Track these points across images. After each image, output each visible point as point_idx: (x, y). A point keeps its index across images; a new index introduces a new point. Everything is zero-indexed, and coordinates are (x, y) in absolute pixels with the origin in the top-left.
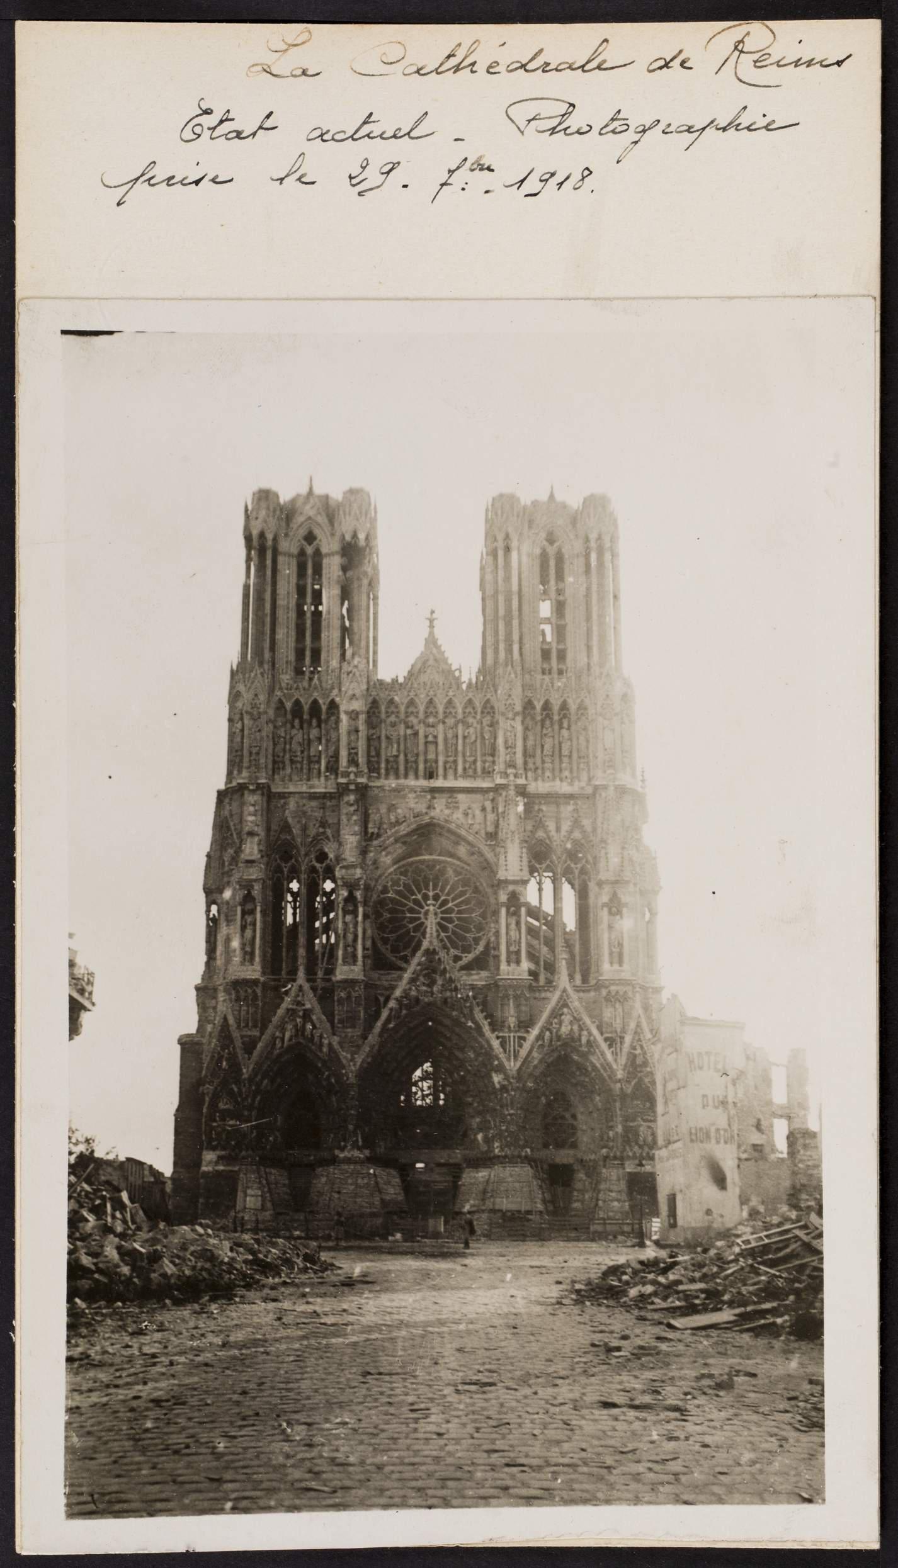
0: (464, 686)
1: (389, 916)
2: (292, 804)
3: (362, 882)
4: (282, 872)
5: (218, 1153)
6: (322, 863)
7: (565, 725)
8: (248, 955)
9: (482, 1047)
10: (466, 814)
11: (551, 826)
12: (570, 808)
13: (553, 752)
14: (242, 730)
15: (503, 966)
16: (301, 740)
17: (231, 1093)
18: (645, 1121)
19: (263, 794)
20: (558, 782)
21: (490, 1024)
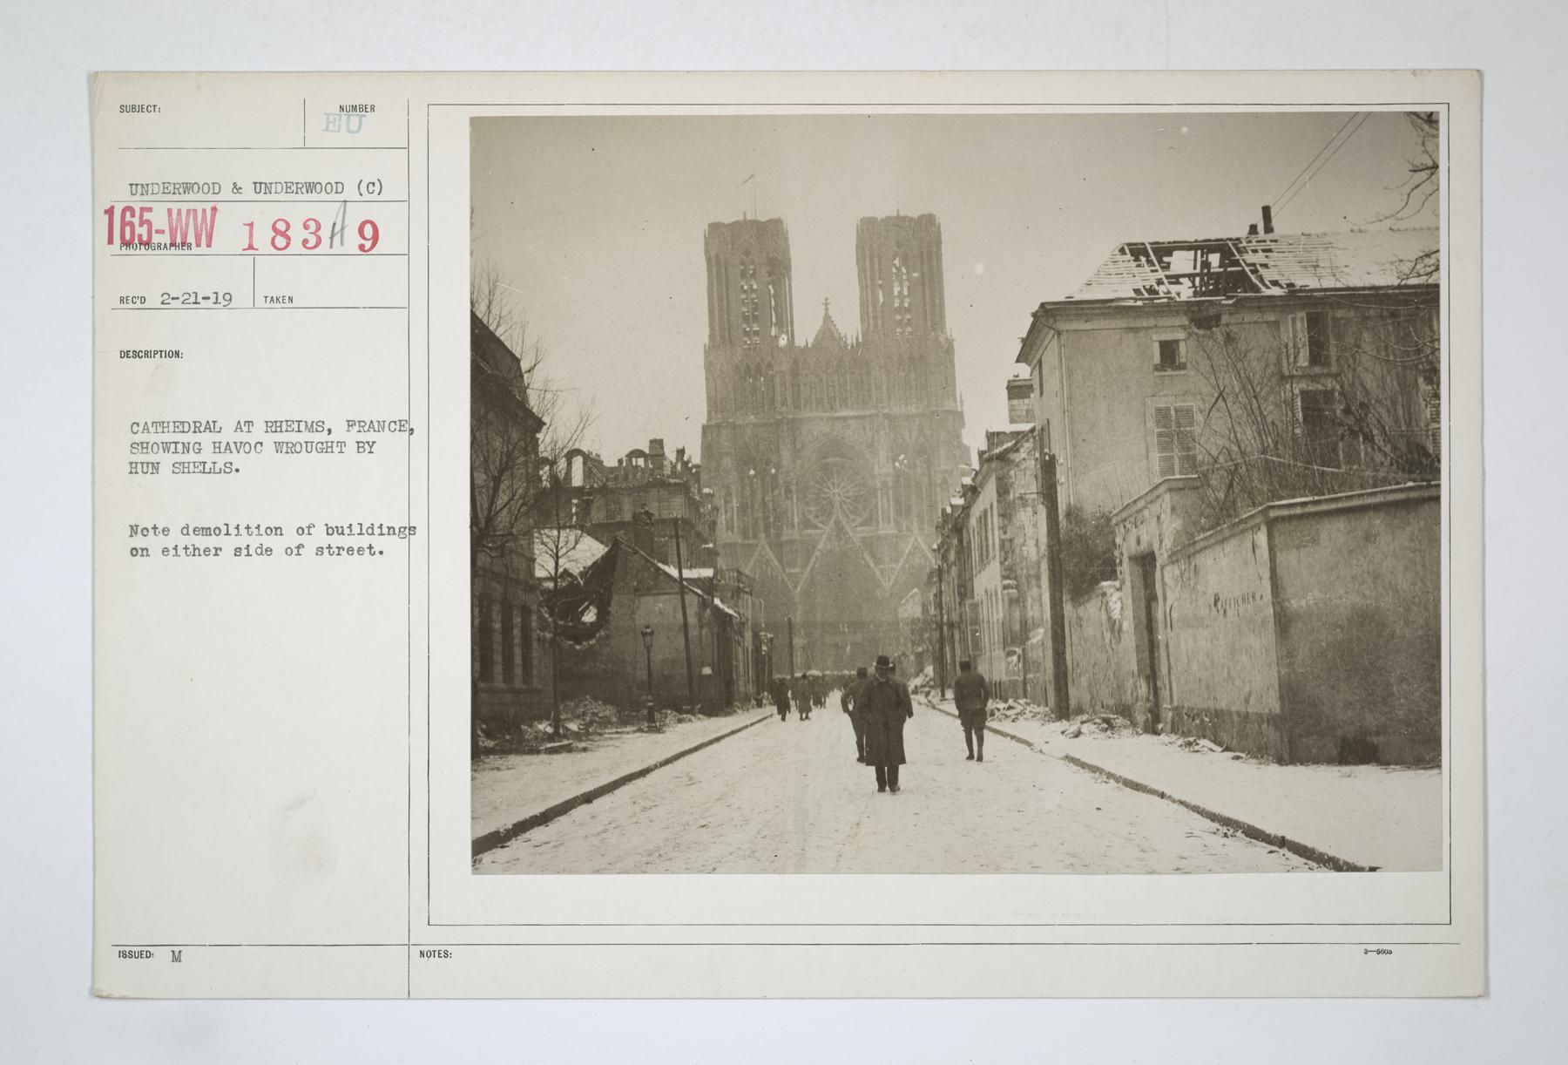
0: (849, 347)
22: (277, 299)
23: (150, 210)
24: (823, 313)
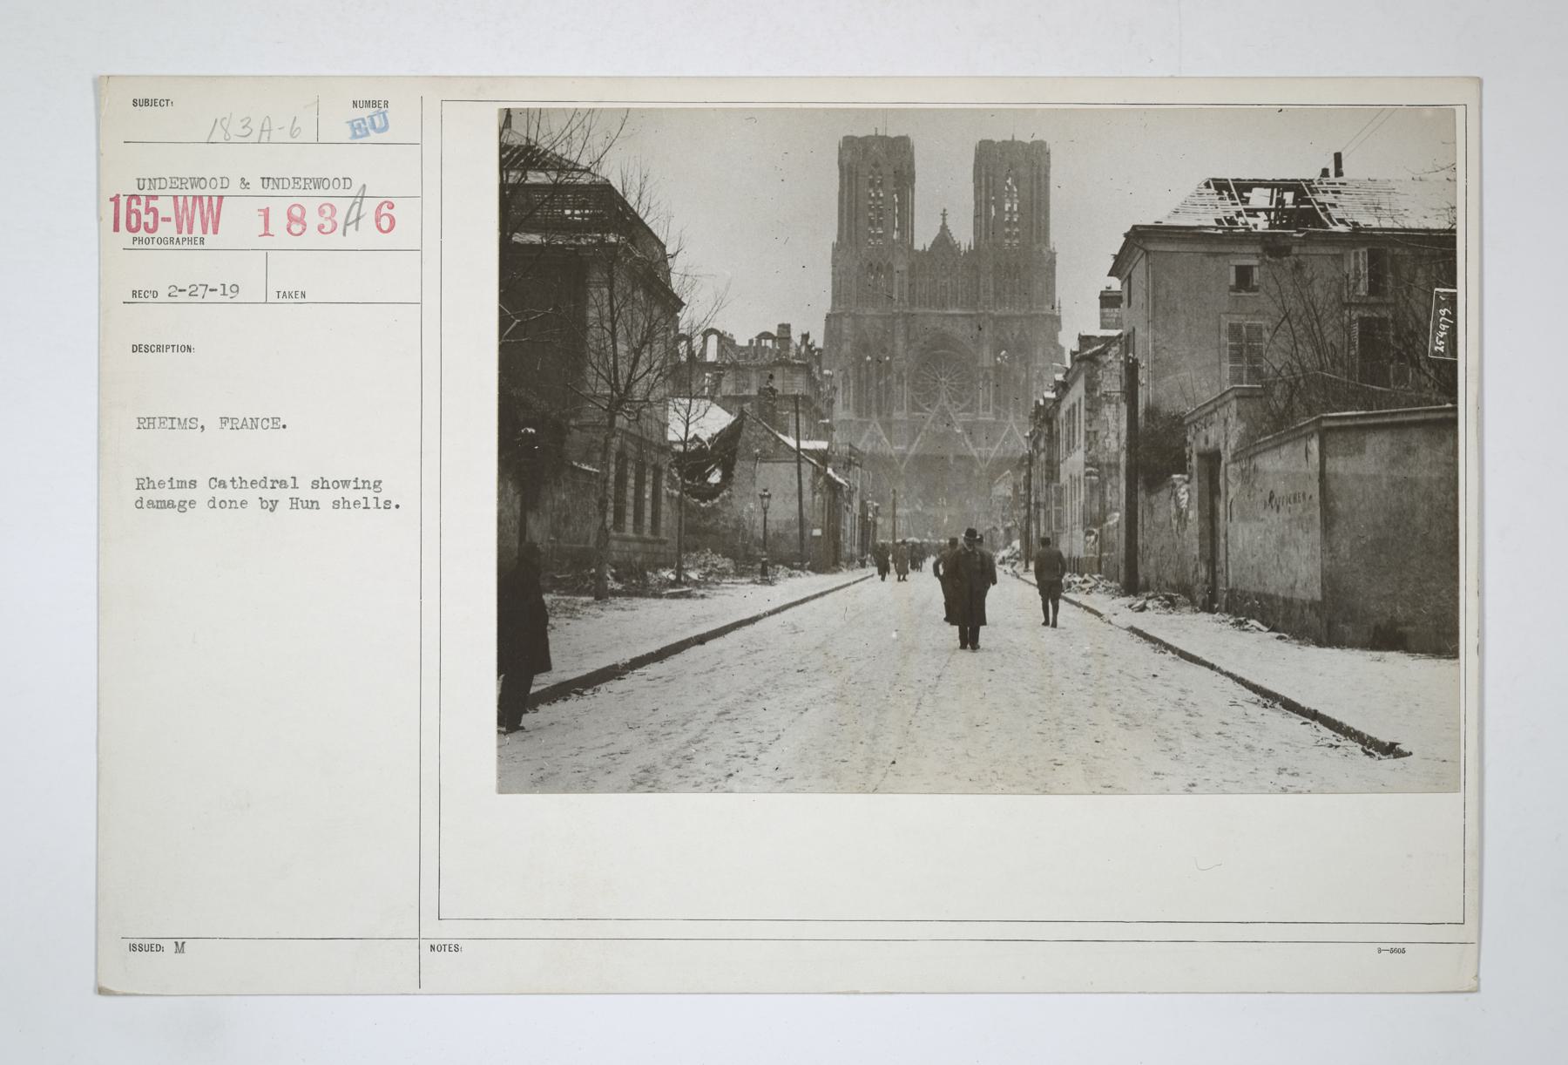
2: (867, 321)
3: (906, 368)
11: (1008, 334)
12: (1019, 324)
14: (840, 281)
22: (290, 295)
23: (155, 197)
24: (941, 223)
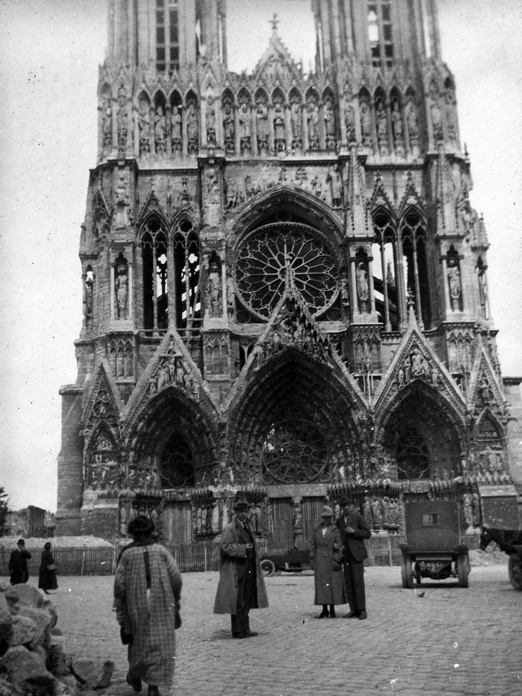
0: (306, 78)
1: (248, 275)
4: (150, 239)
5: (99, 491)
6: (186, 231)
7: (396, 107)
8: (121, 312)
9: (341, 387)
10: (315, 184)
11: (390, 195)
12: (405, 177)
13: (387, 131)
15: (356, 314)
16: (164, 125)
17: (110, 437)
18: (493, 449)
19: (131, 170)
20: (393, 155)
21: (347, 365)
